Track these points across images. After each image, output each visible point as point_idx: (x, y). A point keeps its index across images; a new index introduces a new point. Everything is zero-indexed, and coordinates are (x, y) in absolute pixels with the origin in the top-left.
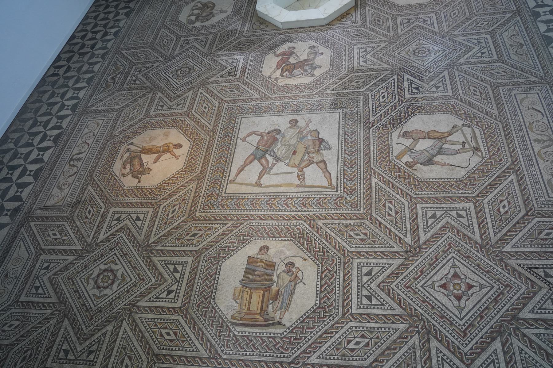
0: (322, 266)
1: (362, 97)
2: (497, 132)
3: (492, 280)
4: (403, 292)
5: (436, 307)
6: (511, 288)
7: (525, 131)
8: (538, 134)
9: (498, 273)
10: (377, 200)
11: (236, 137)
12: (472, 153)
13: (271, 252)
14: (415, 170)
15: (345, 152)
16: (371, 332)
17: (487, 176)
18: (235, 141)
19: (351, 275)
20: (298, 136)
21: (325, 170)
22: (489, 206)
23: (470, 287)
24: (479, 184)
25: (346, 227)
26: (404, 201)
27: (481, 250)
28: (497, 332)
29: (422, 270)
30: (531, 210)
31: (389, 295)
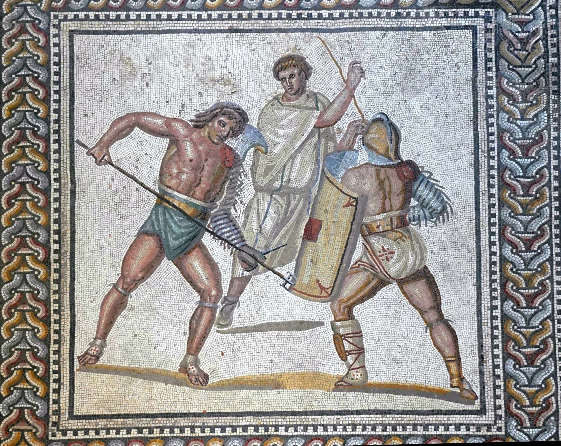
15: (502, 233)
18: (66, 157)
20: (317, 147)
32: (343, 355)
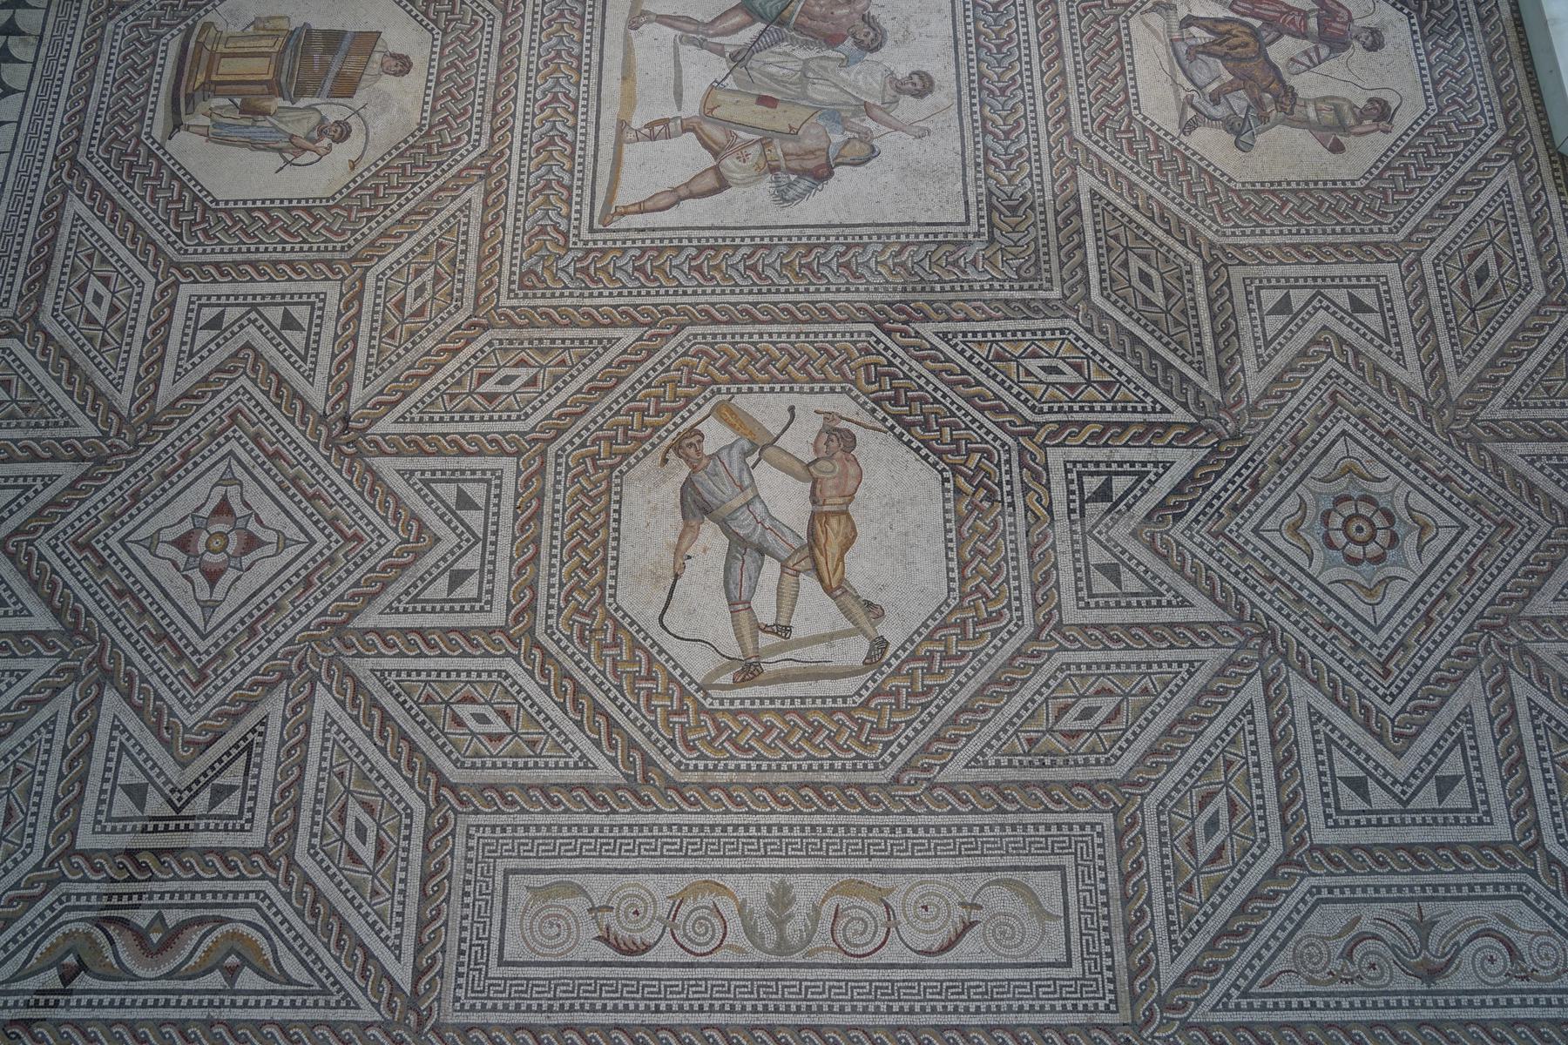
0: (328, 208)
2: (834, 757)
3: (225, 637)
4: (220, 406)
5: (166, 485)
6: (195, 685)
7: (839, 863)
8: (817, 910)
9: (246, 659)
10: (546, 344)
12: (736, 652)
13: (389, 83)
14: (665, 461)
16: (121, 329)
17: (619, 688)
19: (290, 279)
22: (490, 673)
23: (213, 577)
24: (587, 656)
25: (452, 262)
26: (531, 422)
27: (326, 624)
28: (74, 625)
29: (282, 457)
30: (462, 802)
31: (218, 370)
32: (650, 126)
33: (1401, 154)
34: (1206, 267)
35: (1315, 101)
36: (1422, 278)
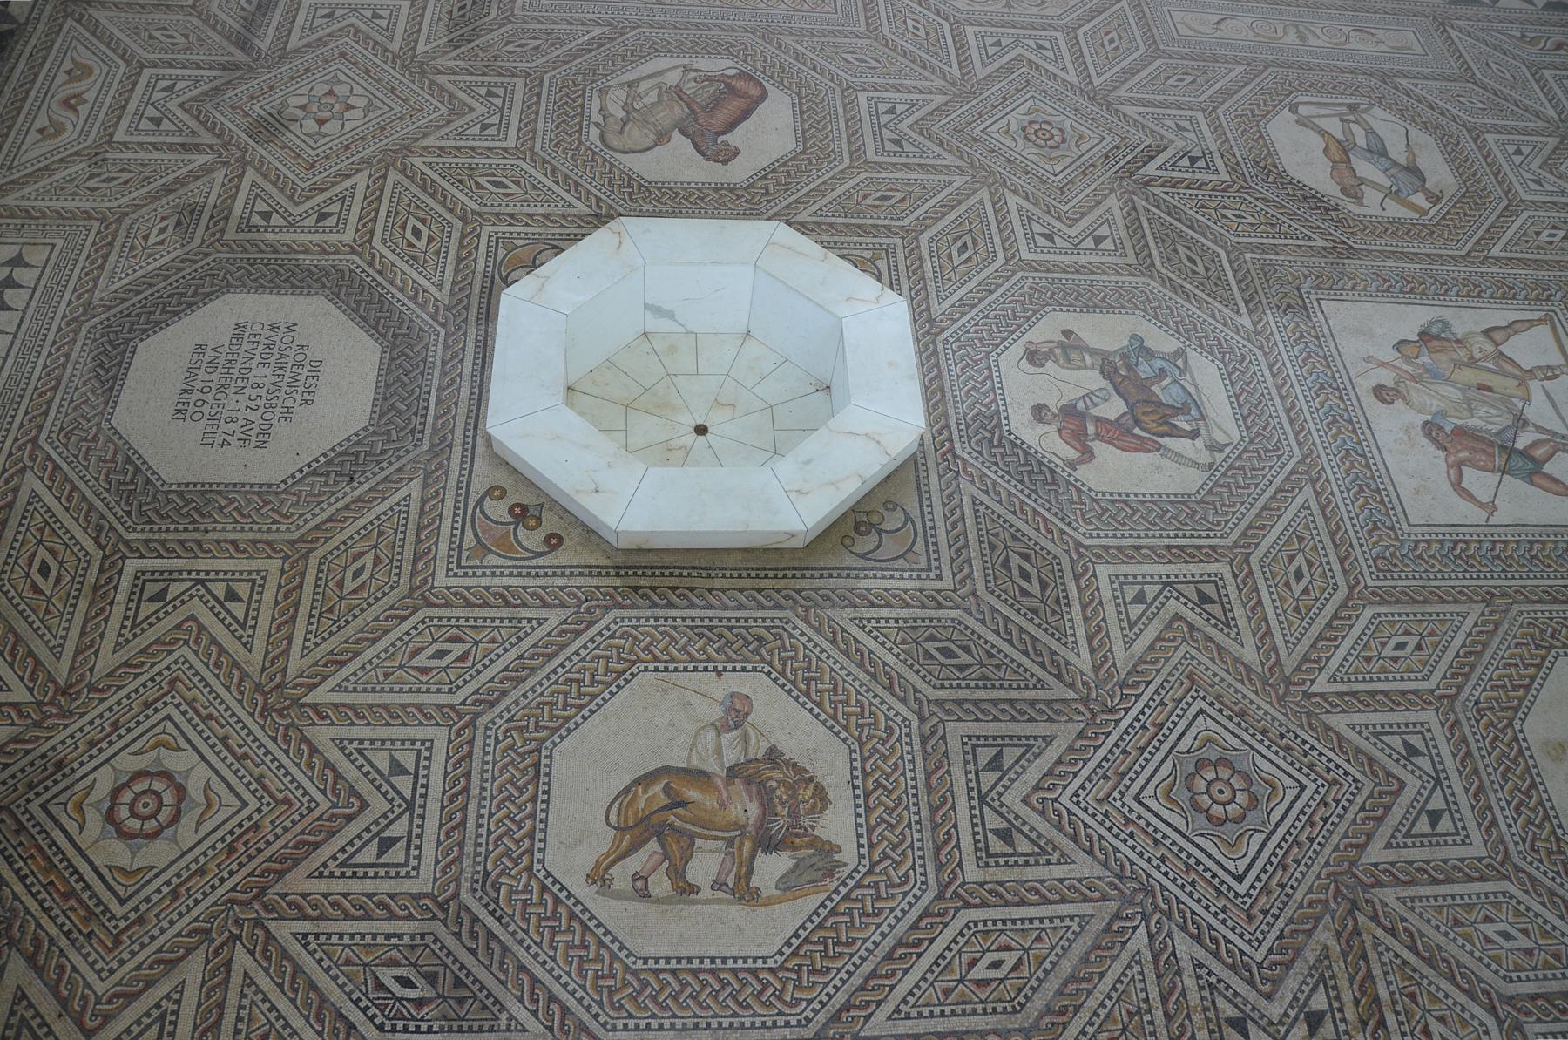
1: (1248, 256)
11: (1486, 530)
21: (1512, 328)
33: (1019, 326)
34: (1153, 265)
35: (1086, 367)
36: (1005, 250)
